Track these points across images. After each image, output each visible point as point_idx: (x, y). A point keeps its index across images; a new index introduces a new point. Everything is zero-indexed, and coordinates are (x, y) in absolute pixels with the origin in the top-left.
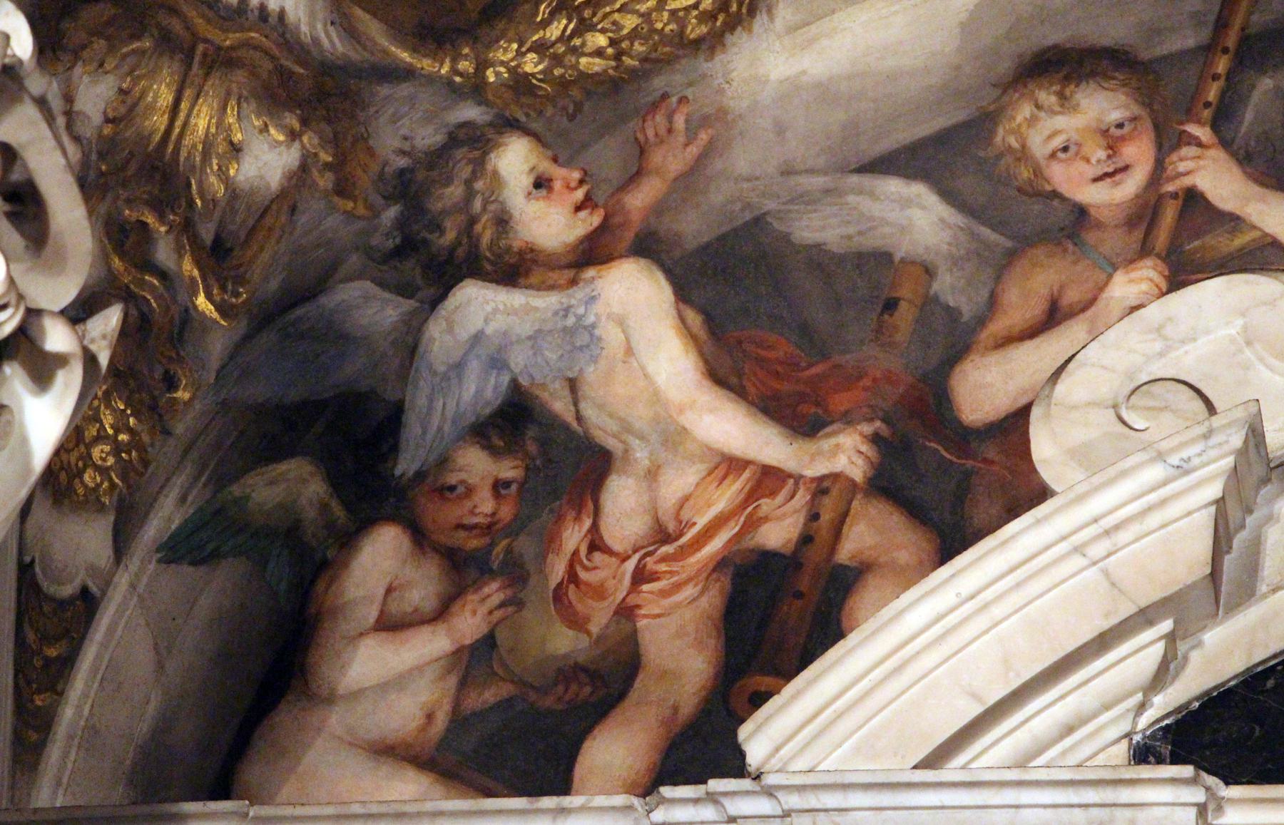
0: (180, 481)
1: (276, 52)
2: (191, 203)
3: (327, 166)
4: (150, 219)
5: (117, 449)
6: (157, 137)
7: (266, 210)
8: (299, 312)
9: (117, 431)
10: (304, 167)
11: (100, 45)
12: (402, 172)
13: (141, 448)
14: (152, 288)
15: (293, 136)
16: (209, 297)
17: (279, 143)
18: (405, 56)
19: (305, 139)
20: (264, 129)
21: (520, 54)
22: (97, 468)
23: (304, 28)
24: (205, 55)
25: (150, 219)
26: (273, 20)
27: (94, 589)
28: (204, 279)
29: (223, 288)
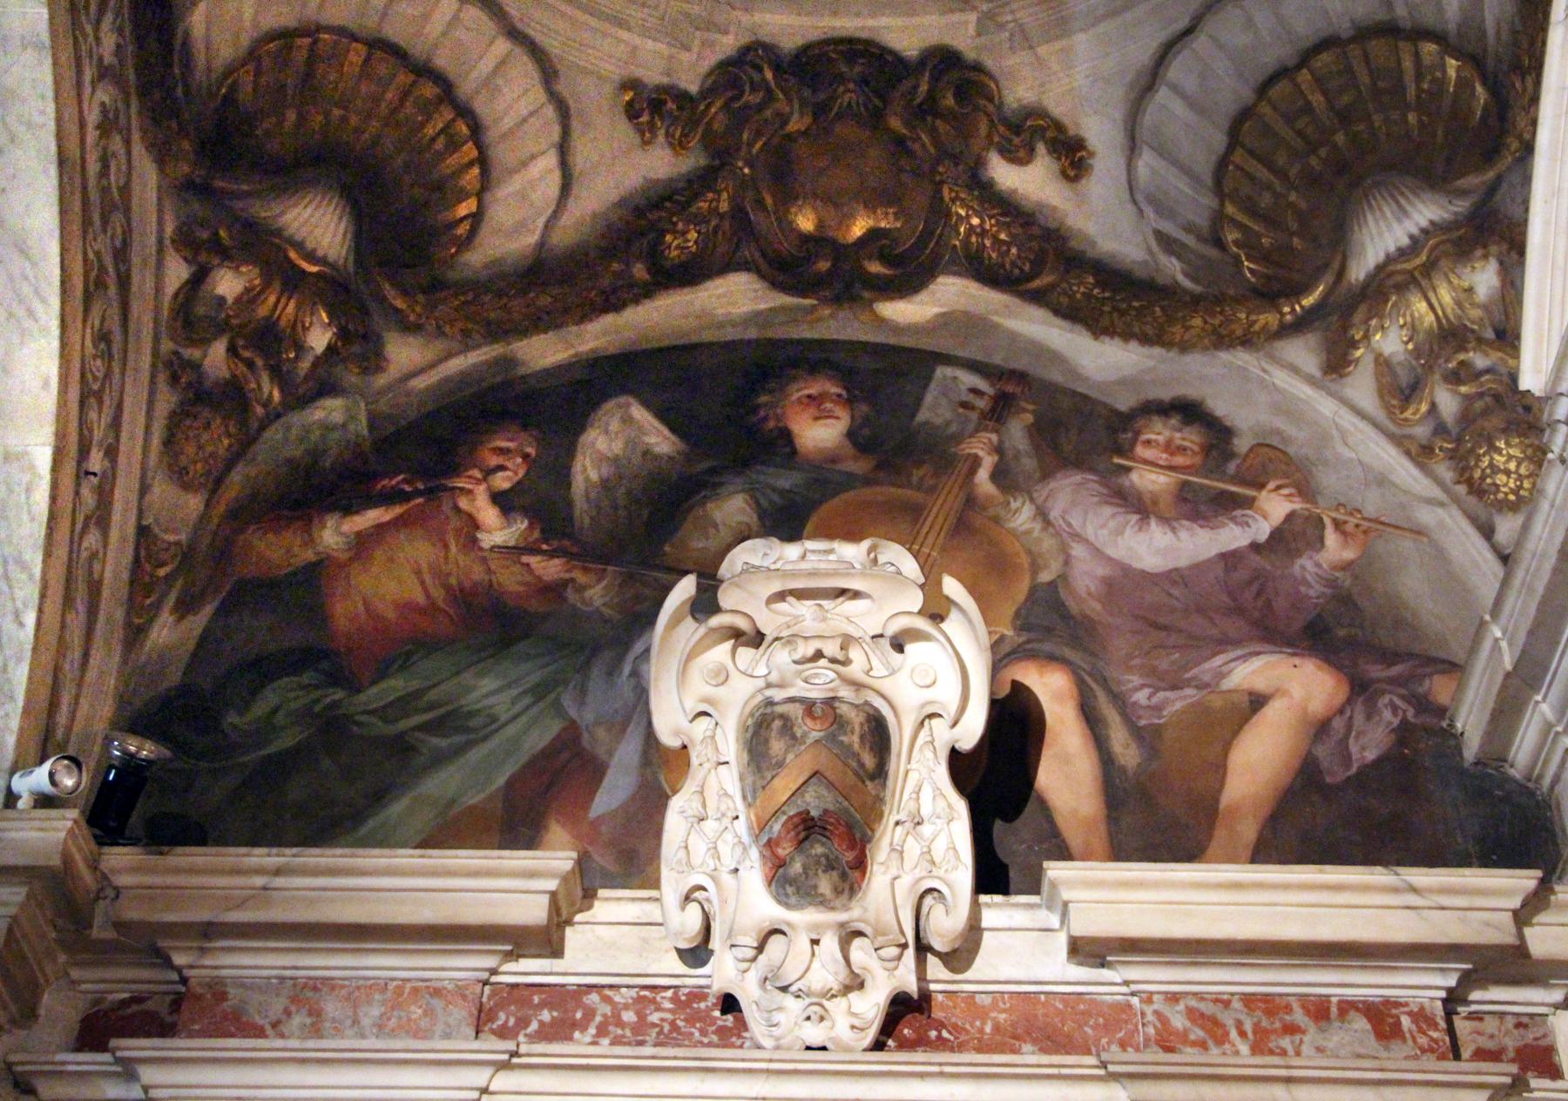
1: (1444, 237)
2: (1473, 331)
4: (1462, 356)
6: (1435, 325)
7: (1503, 297)
10: (1501, 263)
11: (1374, 322)
23: (1446, 216)
26: (1431, 229)
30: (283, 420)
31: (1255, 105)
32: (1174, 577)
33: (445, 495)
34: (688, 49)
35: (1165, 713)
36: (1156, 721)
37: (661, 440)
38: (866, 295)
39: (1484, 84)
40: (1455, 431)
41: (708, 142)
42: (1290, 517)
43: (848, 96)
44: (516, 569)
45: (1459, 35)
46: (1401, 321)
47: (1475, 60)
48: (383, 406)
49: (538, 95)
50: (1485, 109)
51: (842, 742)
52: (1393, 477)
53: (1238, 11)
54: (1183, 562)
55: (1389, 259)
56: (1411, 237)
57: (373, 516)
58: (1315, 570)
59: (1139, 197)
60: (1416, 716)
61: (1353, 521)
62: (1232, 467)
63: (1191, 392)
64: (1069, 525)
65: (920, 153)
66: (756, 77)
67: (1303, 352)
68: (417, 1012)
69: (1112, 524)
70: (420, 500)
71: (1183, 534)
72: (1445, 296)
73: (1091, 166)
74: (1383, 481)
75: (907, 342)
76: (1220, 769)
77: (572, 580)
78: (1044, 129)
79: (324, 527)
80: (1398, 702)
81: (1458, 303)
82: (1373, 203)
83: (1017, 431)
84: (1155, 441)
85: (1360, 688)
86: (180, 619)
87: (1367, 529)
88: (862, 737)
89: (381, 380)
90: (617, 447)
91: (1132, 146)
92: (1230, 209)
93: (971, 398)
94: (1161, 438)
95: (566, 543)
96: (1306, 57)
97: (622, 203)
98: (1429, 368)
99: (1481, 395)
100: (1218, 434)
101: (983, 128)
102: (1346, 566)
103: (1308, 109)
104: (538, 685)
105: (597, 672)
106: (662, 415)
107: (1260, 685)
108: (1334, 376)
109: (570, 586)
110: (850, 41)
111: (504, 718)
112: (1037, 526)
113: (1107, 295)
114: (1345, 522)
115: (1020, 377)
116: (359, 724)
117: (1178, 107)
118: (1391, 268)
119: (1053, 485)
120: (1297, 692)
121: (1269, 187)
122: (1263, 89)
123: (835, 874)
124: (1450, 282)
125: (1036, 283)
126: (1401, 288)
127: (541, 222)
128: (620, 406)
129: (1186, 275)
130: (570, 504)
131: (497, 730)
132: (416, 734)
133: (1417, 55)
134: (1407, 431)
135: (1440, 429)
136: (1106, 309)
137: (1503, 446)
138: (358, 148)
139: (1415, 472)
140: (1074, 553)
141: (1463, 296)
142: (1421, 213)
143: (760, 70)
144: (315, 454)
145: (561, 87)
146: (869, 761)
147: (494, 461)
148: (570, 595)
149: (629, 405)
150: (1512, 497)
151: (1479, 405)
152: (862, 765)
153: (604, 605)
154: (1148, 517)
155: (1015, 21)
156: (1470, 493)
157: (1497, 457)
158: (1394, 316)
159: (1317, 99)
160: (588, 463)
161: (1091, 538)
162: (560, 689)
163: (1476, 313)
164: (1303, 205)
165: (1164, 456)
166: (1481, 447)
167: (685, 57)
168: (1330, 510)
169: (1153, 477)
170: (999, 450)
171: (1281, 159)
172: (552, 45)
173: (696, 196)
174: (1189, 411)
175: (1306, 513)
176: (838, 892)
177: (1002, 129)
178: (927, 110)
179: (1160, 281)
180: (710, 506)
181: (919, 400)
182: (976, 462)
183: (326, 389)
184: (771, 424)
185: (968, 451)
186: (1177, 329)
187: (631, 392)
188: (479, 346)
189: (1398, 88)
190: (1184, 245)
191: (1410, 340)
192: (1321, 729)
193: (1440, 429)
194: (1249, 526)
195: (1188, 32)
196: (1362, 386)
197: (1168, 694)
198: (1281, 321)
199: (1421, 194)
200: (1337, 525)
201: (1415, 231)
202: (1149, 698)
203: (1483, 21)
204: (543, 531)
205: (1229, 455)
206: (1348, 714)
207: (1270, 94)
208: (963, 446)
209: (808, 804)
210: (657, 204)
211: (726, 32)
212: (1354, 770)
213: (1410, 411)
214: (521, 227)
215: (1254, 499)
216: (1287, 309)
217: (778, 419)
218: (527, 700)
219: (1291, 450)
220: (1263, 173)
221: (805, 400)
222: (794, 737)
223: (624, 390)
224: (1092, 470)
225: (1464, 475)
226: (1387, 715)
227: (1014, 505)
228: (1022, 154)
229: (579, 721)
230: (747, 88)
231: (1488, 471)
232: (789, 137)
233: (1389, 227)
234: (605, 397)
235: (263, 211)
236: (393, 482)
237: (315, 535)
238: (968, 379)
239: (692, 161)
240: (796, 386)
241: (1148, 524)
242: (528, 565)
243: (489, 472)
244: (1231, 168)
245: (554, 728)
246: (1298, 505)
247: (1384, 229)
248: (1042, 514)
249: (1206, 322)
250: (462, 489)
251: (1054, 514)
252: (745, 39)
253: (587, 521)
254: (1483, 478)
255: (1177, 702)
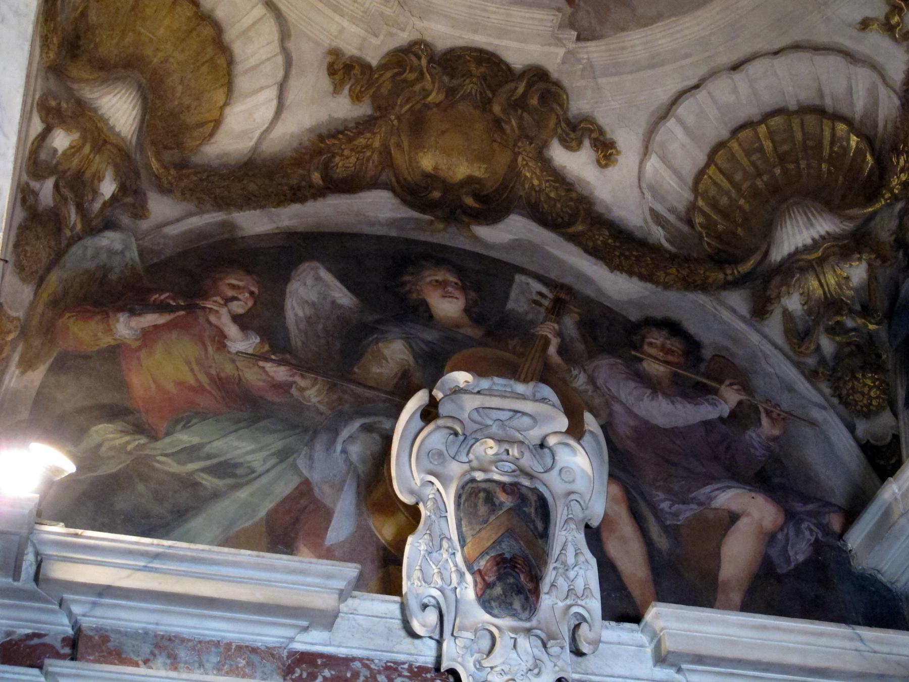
0: (898, 382)
1: (834, 243)
2: (847, 304)
3: (876, 258)
4: (839, 318)
5: (878, 388)
6: (823, 296)
7: (869, 286)
8: (897, 305)
9: (874, 383)
10: (870, 265)
11: (784, 289)
12: (895, 240)
13: (884, 382)
14: (854, 336)
15: (860, 260)
16: (871, 323)
17: (858, 265)
18: (870, 210)
19: (864, 257)
20: (851, 266)
21: (898, 178)
22: (874, 398)
24: (817, 263)
25: (839, 318)
27: (896, 433)
28: (866, 320)
29: (874, 318)
30: (82, 242)
31: (728, 141)
32: (674, 433)
33: (200, 313)
34: (376, 36)
35: (681, 518)
36: (676, 523)
37: (343, 297)
38: (466, 219)
39: (873, 155)
40: (831, 364)
41: (374, 98)
42: (740, 403)
43: (470, 87)
44: (256, 369)
45: (861, 121)
46: (801, 292)
47: (869, 140)
48: (147, 243)
49: (275, 47)
50: (871, 169)
51: (525, 512)
52: (796, 387)
53: (730, 81)
54: (681, 423)
55: (797, 252)
56: (813, 239)
57: (151, 319)
58: (758, 439)
59: (644, 186)
60: (822, 537)
61: (776, 411)
62: (703, 367)
63: (674, 315)
64: (609, 390)
65: (508, 131)
66: (415, 61)
67: (738, 300)
68: (242, 663)
69: (635, 393)
70: (182, 313)
71: (679, 406)
72: (831, 280)
73: (617, 161)
74: (791, 389)
75: (494, 254)
76: (717, 556)
77: (295, 382)
78: (591, 131)
79: (118, 321)
80: (812, 527)
81: (839, 285)
82: (792, 215)
83: (570, 323)
84: (655, 343)
85: (790, 516)
86: (23, 373)
87: (784, 418)
88: (536, 509)
89: (145, 225)
90: (313, 297)
91: (646, 152)
92: (700, 203)
93: (538, 298)
94: (658, 342)
95: (288, 356)
96: (766, 117)
97: (311, 130)
98: (816, 323)
99: (848, 344)
100: (692, 346)
101: (552, 123)
102: (775, 439)
103: (761, 149)
104: (279, 451)
105: (319, 447)
106: (343, 278)
107: (735, 507)
108: (758, 319)
109: (294, 386)
110: (480, 51)
111: (260, 470)
112: (590, 388)
113: (617, 244)
114: (772, 411)
115: (568, 289)
116: (159, 462)
117: (679, 132)
118: (798, 257)
119: (596, 363)
120: (756, 514)
121: (727, 193)
122: (735, 132)
123: (522, 596)
124: (835, 271)
125: (572, 230)
126: (802, 270)
127: (257, 134)
128: (312, 269)
129: (667, 240)
130: (286, 330)
131: (255, 478)
132: (202, 474)
133: (833, 129)
134: (802, 360)
135: (822, 361)
136: (617, 253)
137: (860, 377)
138: (155, 60)
139: (807, 385)
140: (614, 408)
141: (843, 282)
142: (821, 226)
143: (419, 58)
144: (105, 270)
145: (291, 45)
146: (540, 526)
147: (230, 293)
148: (294, 391)
149: (318, 268)
150: (865, 409)
151: (847, 350)
152: (536, 528)
153: (319, 402)
154: (657, 392)
155: (588, 59)
156: (840, 403)
157: (856, 383)
158: (797, 286)
159: (768, 145)
160: (295, 305)
161: (624, 400)
162: (295, 455)
163: (850, 293)
164: (747, 207)
165: (661, 354)
166: (847, 376)
167: (376, 41)
168: (762, 402)
169: (657, 366)
170: (559, 334)
171: (738, 177)
172: (292, 16)
173: (360, 134)
174: (673, 327)
175: (749, 402)
176: (524, 608)
177: (563, 125)
178: (518, 105)
179: (651, 241)
180: (380, 345)
181: (507, 297)
182: (547, 342)
183: (110, 225)
184: (414, 296)
185: (541, 333)
186: (661, 274)
187: (318, 260)
188: (208, 212)
189: (819, 146)
190: (668, 221)
191: (806, 303)
192: (771, 538)
193: (822, 361)
194: (717, 406)
195: (696, 87)
196: (774, 326)
197: (681, 506)
198: (725, 278)
199: (824, 215)
200: (768, 413)
201: (816, 236)
202: (670, 507)
203: (877, 116)
204: (270, 346)
205: (700, 360)
206: (786, 531)
207: (739, 135)
208: (538, 329)
209: (504, 549)
210: (333, 136)
211: (403, 30)
212: (793, 566)
213: (804, 347)
214: (245, 134)
215: (718, 389)
216: (729, 272)
217: (419, 293)
218: (273, 461)
219: (736, 361)
220: (726, 184)
221: (435, 283)
222: (494, 504)
223: (312, 258)
224: (620, 357)
225: (837, 392)
226: (807, 533)
227: (575, 372)
228: (574, 144)
229: (310, 479)
230: (408, 68)
231: (851, 391)
232: (427, 107)
233: (800, 232)
234: (301, 260)
235: (89, 93)
236: (162, 297)
237: (112, 327)
238: (537, 286)
239: (364, 109)
240: (427, 273)
241: (657, 396)
242: (263, 368)
243: (229, 300)
244: (706, 177)
245: (294, 482)
246: (744, 398)
247: (797, 231)
248: (592, 381)
249: (678, 271)
250: (211, 309)
251: (600, 382)
252: (415, 36)
253: (299, 344)
254: (848, 395)
255: (687, 512)
